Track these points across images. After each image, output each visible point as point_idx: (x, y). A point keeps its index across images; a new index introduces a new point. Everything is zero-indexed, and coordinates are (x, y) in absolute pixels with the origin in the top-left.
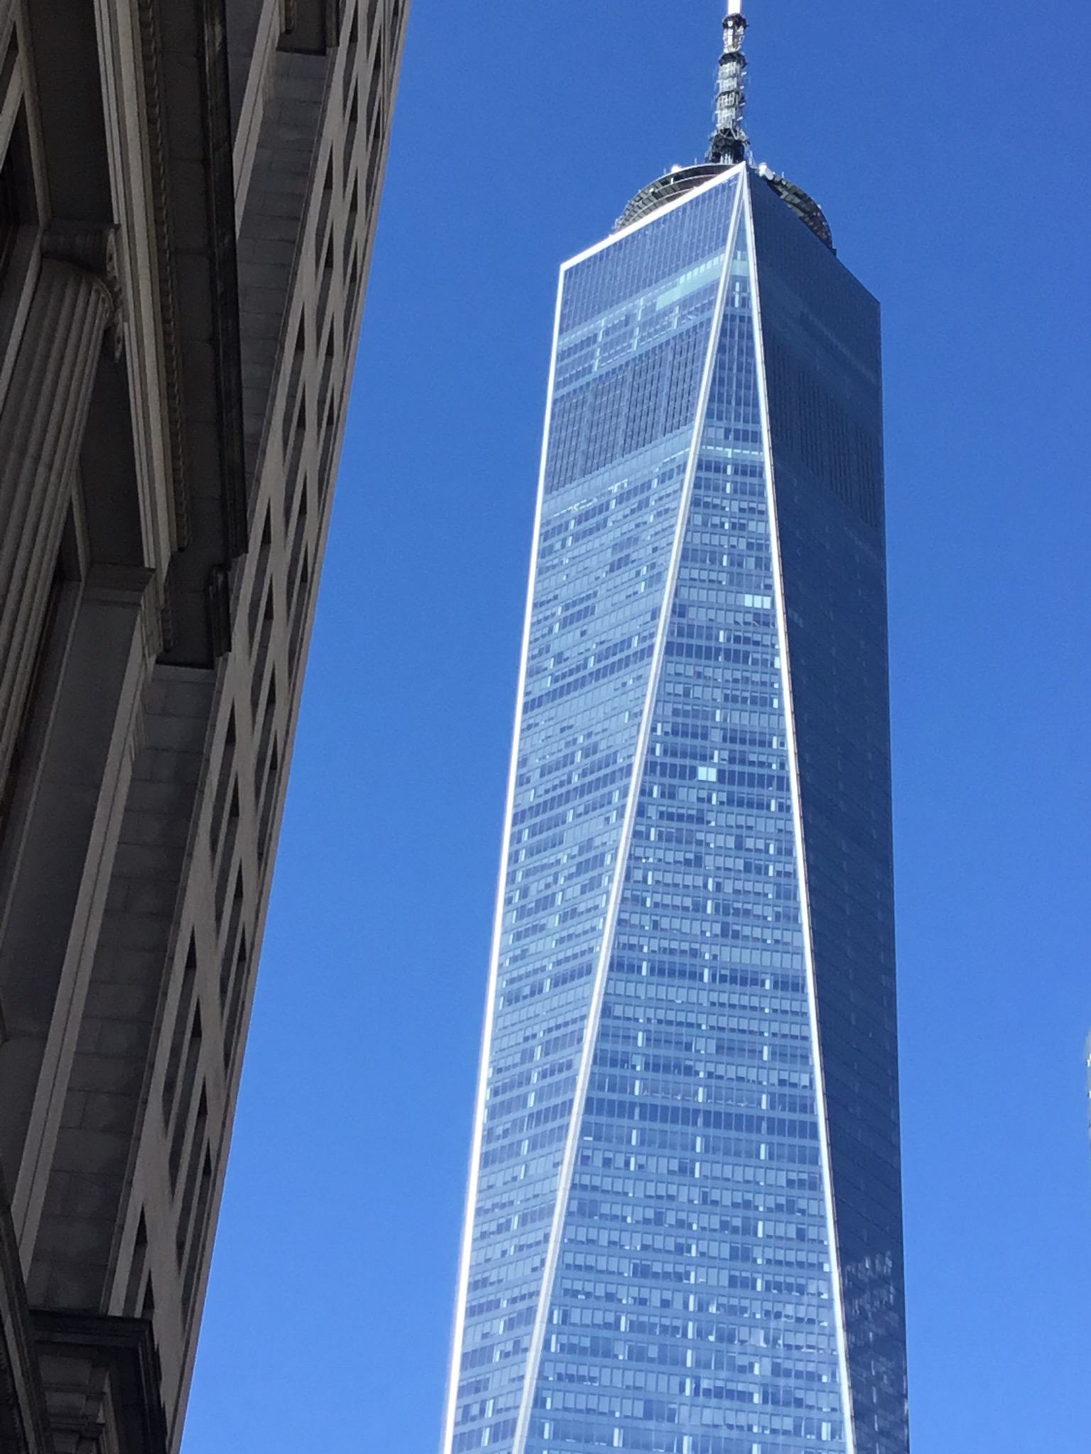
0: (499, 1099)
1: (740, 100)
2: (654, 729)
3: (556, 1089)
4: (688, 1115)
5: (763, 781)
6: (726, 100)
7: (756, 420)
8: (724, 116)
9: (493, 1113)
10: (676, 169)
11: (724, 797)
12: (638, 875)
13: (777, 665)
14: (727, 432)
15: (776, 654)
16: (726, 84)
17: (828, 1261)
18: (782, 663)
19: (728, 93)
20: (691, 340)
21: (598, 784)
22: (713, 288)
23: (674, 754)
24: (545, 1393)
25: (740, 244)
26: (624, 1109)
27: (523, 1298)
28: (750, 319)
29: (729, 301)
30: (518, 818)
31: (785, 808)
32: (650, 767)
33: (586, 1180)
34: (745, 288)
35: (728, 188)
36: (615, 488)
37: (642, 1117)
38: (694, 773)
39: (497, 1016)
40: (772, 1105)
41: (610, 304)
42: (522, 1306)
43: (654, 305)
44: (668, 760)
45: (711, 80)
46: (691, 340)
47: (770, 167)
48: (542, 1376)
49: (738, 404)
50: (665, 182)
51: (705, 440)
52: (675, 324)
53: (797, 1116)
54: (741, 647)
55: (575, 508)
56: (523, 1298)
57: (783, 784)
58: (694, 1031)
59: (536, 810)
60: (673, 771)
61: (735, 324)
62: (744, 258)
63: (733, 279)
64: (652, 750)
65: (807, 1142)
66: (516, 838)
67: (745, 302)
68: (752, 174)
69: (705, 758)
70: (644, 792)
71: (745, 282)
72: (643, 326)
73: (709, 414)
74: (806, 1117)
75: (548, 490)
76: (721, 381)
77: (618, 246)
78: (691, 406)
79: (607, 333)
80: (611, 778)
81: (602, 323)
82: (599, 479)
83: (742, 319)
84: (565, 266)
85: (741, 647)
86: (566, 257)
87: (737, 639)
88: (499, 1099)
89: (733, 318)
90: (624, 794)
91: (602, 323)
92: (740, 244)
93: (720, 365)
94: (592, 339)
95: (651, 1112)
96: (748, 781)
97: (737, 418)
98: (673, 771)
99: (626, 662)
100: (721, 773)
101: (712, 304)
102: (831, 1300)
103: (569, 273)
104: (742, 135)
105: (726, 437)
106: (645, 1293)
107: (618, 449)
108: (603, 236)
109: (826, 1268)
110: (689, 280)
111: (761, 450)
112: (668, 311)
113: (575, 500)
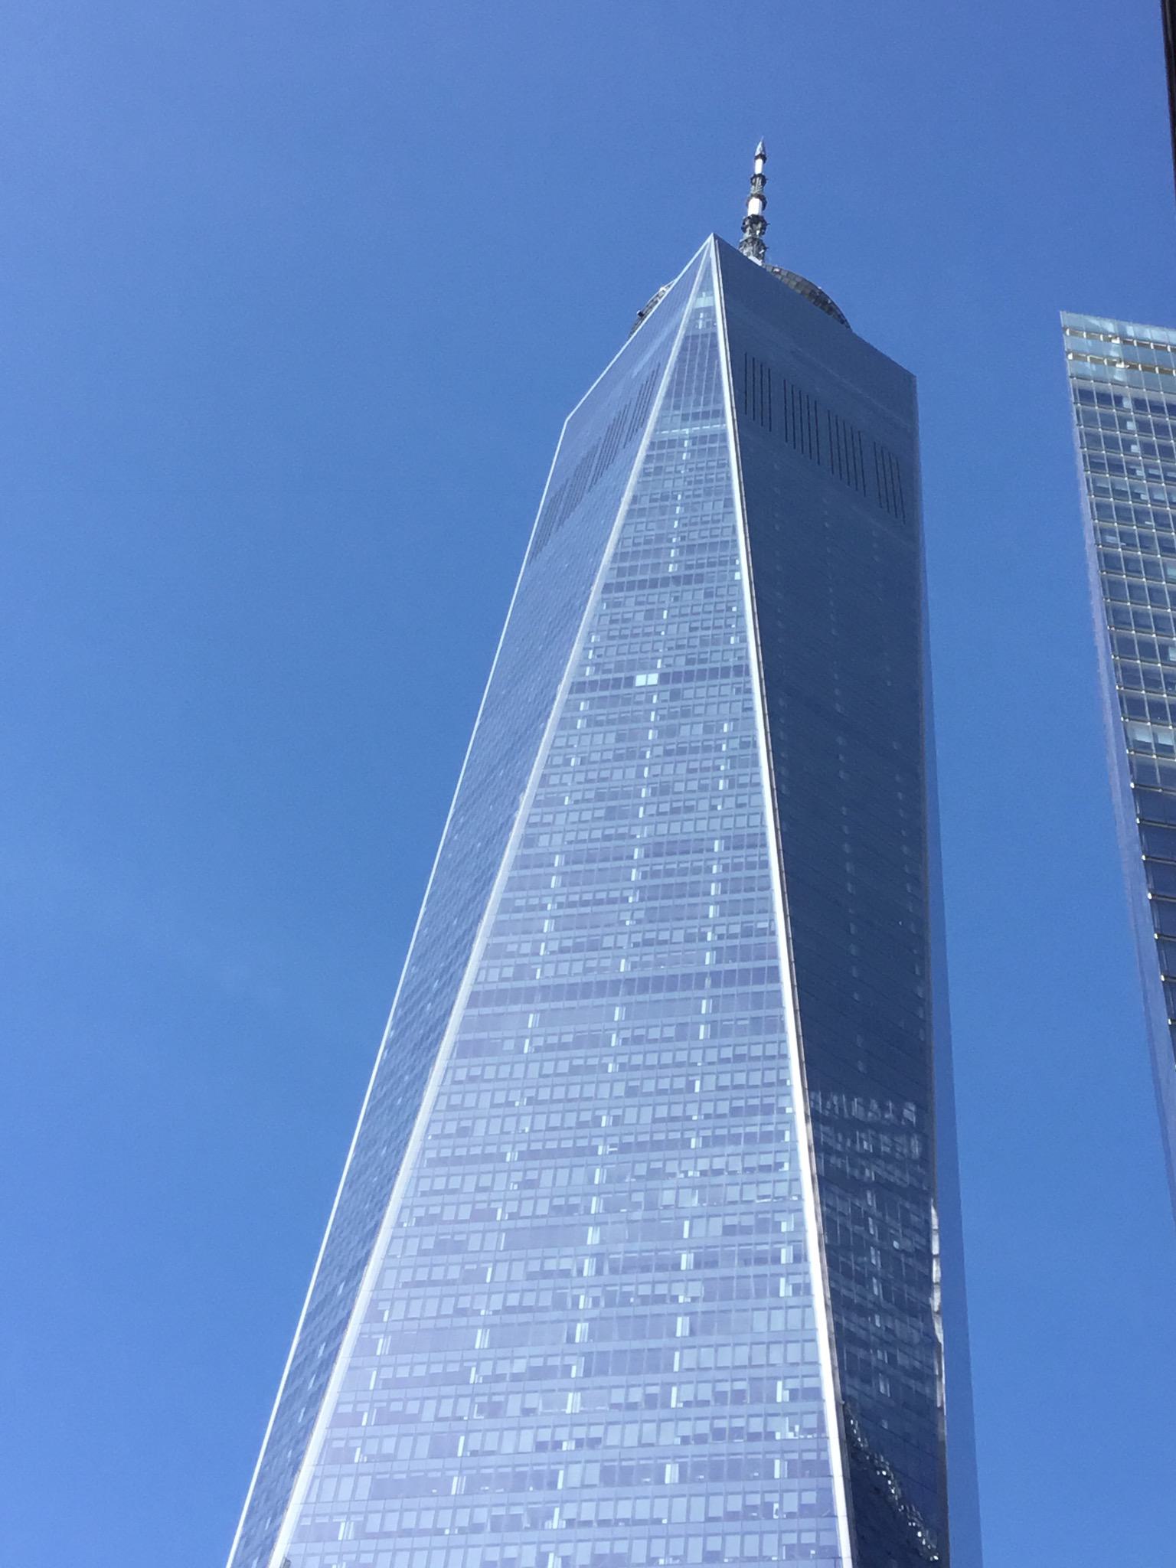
7: (719, 400)
11: (667, 696)
12: (554, 780)
13: (737, 576)
15: (739, 569)
17: (791, 1104)
24: (382, 1306)
28: (715, 335)
32: (578, 687)
38: (630, 681)
49: (699, 393)
52: (648, 373)
57: (743, 670)
60: (605, 685)
63: (696, 312)
65: (771, 987)
67: (712, 324)
69: (647, 668)
71: (710, 311)
73: (665, 408)
76: (680, 383)
83: (706, 335)
87: (690, 567)
89: (695, 337)
92: (706, 286)
97: (697, 403)
98: (605, 685)
100: (664, 678)
105: (685, 417)
106: (532, 1175)
109: (789, 1110)
111: (724, 422)
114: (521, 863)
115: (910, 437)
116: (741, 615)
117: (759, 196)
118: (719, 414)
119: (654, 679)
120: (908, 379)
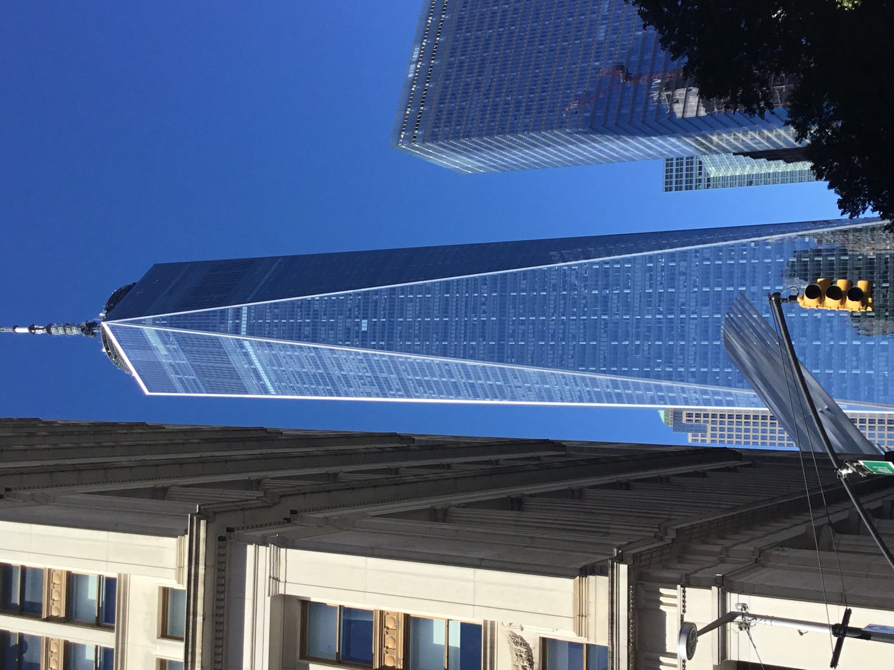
0: (498, 394)
1: (66, 325)
2: (348, 345)
3: (495, 375)
4: (502, 323)
5: (366, 302)
6: (68, 331)
7: (215, 311)
8: (75, 331)
9: (504, 398)
10: (104, 350)
14: (221, 323)
15: (313, 298)
16: (61, 332)
18: (317, 297)
19: (65, 330)
20: (182, 340)
21: (371, 366)
22: (157, 332)
23: (383, 337)
25: (139, 322)
26: (501, 348)
27: (575, 382)
28: (171, 316)
29: (164, 325)
30: (385, 396)
31: (376, 292)
32: (364, 346)
33: (530, 360)
34: (158, 319)
35: (113, 329)
36: (246, 366)
37: (503, 340)
39: (467, 399)
40: (495, 292)
41: (164, 373)
42: (579, 382)
43: (165, 356)
44: (386, 339)
45: (59, 337)
46: (182, 340)
47: (101, 312)
48: (604, 372)
50: (109, 354)
51: (225, 332)
53: (499, 282)
54: (311, 313)
55: (255, 382)
56: (575, 382)
58: (468, 323)
59: (381, 389)
61: (173, 323)
62: (145, 320)
64: (357, 346)
66: (393, 396)
67: (164, 319)
68: (105, 320)
69: (359, 325)
70: (374, 347)
71: (154, 319)
72: (175, 359)
73: (214, 331)
74: (499, 278)
75: (246, 393)
77: (138, 371)
78: (210, 338)
79: (177, 373)
80: (368, 361)
81: (173, 376)
82: (241, 372)
84: (147, 393)
85: (311, 313)
86: (142, 392)
88: (498, 394)
90: (375, 355)
91: (173, 376)
93: (192, 328)
94: (180, 380)
95: (501, 338)
96: (367, 307)
99: (320, 358)
100: (364, 318)
101: (166, 333)
102: (567, 266)
103: (150, 391)
104: (84, 324)
106: (570, 335)
107: (229, 366)
108: (134, 378)
110: (155, 341)
112: (168, 350)
113: (249, 381)
114: (444, 355)
115: (195, 266)
116: (339, 295)
117: (14, 328)
118: (222, 311)
119: (365, 322)
120: (156, 266)
